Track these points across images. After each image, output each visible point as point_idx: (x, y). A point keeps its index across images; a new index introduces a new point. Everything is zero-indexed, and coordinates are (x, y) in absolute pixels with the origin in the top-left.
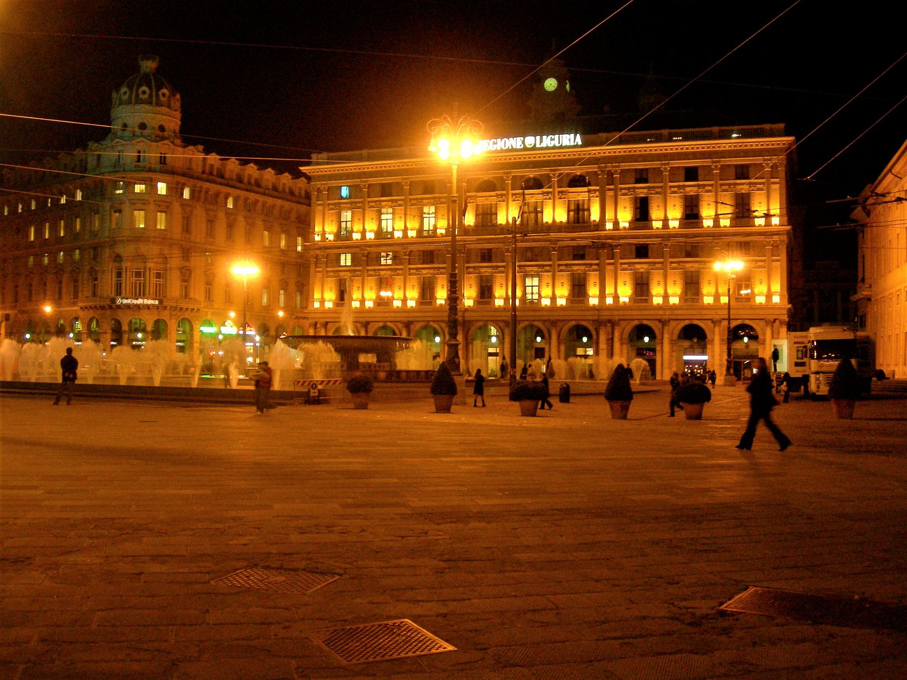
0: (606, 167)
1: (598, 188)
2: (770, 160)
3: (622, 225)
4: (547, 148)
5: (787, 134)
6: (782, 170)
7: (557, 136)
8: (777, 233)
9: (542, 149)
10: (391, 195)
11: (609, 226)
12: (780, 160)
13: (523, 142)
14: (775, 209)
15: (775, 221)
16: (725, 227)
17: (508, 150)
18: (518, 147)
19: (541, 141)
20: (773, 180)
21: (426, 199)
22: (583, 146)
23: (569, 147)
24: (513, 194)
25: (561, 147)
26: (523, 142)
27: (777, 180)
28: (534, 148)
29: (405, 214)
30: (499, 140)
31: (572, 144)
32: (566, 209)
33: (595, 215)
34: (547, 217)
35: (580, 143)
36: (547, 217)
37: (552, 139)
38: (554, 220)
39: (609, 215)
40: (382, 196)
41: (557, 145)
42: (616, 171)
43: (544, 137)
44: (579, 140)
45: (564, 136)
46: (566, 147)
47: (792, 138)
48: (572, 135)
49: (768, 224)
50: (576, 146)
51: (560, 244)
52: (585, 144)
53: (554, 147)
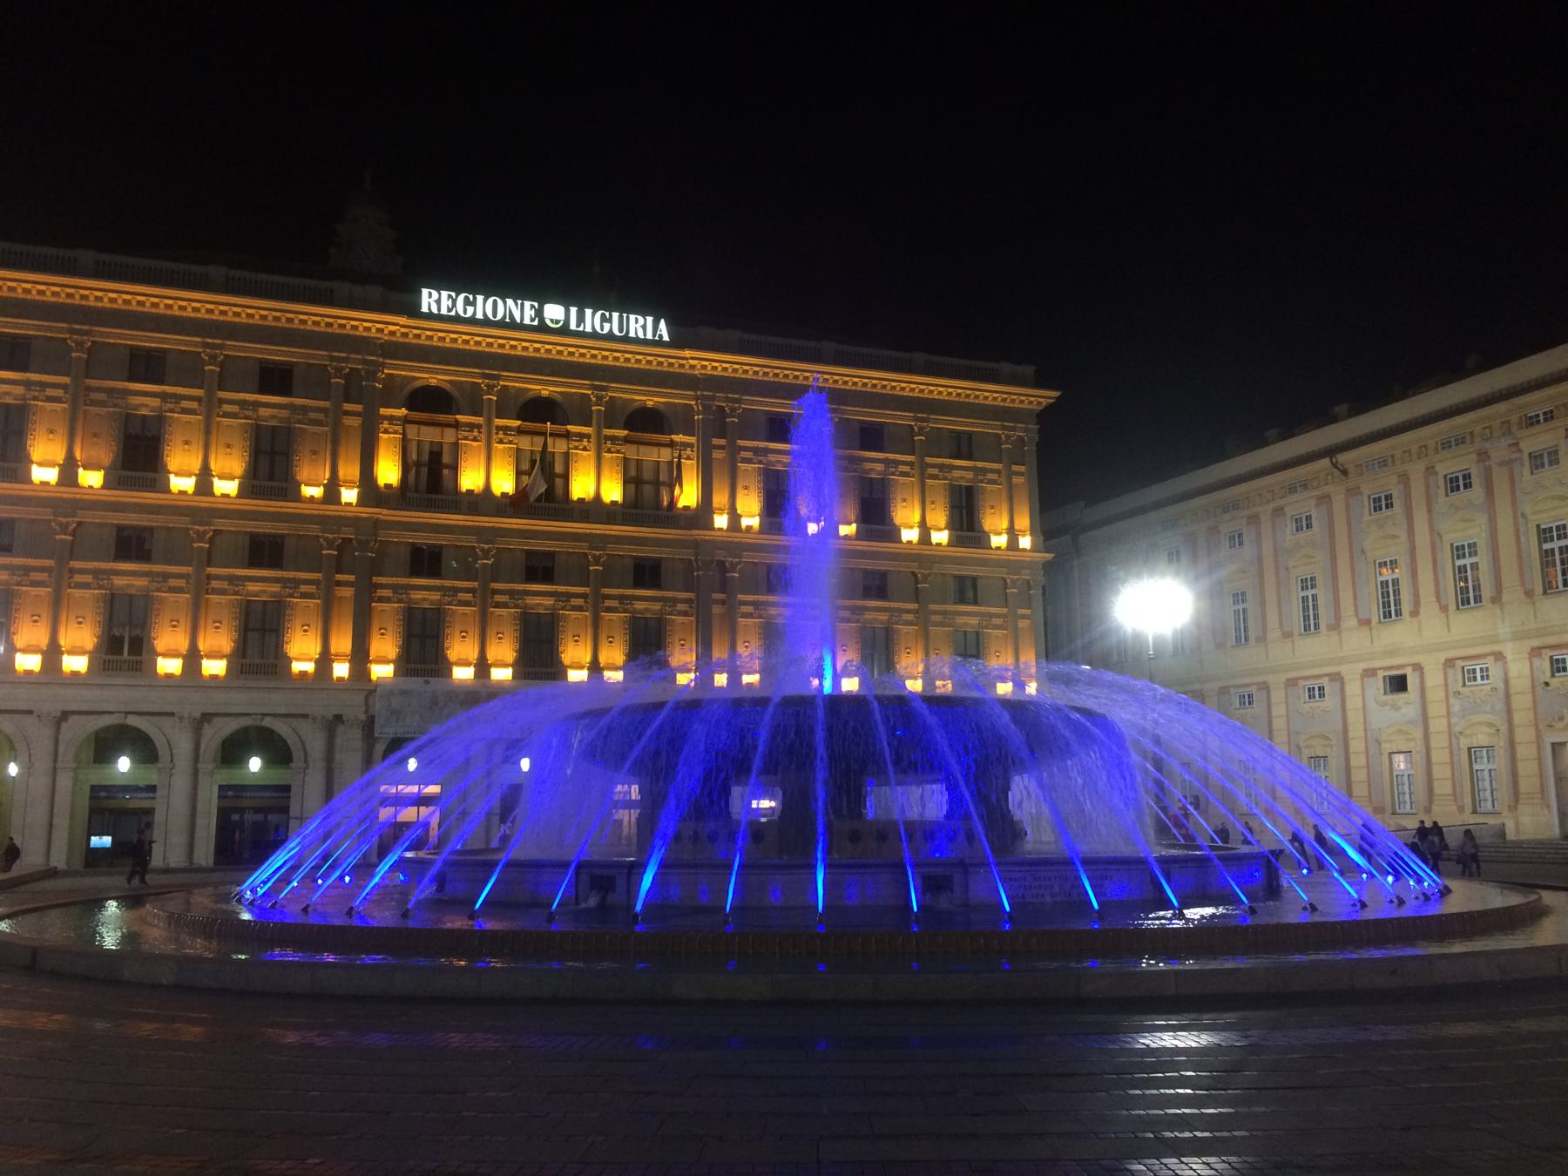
0: (713, 398)
1: (692, 440)
2: (1014, 429)
3: (745, 522)
4: (594, 335)
5: (1039, 383)
6: (1030, 449)
7: (616, 315)
8: (1030, 565)
9: (583, 335)
10: (161, 382)
11: (721, 521)
12: (1027, 433)
13: (539, 313)
14: (1023, 522)
15: (1025, 542)
16: (939, 545)
17: (501, 324)
18: (527, 321)
19: (581, 319)
20: (1015, 468)
21: (267, 405)
22: (676, 343)
23: (645, 342)
24: (499, 428)
25: (626, 339)
26: (539, 313)
27: (1022, 469)
28: (564, 330)
29: (208, 433)
30: (480, 298)
31: (649, 336)
32: (620, 476)
33: (688, 495)
34: (582, 486)
35: (666, 338)
36: (582, 486)
37: (604, 319)
38: (598, 496)
39: (720, 498)
40: (131, 379)
41: (616, 332)
42: (733, 410)
43: (588, 312)
44: (664, 331)
45: (632, 317)
46: (636, 341)
47: (1056, 394)
48: (650, 319)
49: (1013, 544)
50: (659, 343)
51: (613, 550)
52: (676, 343)
53: (610, 337)
